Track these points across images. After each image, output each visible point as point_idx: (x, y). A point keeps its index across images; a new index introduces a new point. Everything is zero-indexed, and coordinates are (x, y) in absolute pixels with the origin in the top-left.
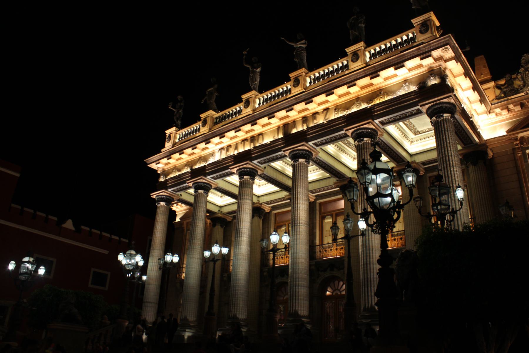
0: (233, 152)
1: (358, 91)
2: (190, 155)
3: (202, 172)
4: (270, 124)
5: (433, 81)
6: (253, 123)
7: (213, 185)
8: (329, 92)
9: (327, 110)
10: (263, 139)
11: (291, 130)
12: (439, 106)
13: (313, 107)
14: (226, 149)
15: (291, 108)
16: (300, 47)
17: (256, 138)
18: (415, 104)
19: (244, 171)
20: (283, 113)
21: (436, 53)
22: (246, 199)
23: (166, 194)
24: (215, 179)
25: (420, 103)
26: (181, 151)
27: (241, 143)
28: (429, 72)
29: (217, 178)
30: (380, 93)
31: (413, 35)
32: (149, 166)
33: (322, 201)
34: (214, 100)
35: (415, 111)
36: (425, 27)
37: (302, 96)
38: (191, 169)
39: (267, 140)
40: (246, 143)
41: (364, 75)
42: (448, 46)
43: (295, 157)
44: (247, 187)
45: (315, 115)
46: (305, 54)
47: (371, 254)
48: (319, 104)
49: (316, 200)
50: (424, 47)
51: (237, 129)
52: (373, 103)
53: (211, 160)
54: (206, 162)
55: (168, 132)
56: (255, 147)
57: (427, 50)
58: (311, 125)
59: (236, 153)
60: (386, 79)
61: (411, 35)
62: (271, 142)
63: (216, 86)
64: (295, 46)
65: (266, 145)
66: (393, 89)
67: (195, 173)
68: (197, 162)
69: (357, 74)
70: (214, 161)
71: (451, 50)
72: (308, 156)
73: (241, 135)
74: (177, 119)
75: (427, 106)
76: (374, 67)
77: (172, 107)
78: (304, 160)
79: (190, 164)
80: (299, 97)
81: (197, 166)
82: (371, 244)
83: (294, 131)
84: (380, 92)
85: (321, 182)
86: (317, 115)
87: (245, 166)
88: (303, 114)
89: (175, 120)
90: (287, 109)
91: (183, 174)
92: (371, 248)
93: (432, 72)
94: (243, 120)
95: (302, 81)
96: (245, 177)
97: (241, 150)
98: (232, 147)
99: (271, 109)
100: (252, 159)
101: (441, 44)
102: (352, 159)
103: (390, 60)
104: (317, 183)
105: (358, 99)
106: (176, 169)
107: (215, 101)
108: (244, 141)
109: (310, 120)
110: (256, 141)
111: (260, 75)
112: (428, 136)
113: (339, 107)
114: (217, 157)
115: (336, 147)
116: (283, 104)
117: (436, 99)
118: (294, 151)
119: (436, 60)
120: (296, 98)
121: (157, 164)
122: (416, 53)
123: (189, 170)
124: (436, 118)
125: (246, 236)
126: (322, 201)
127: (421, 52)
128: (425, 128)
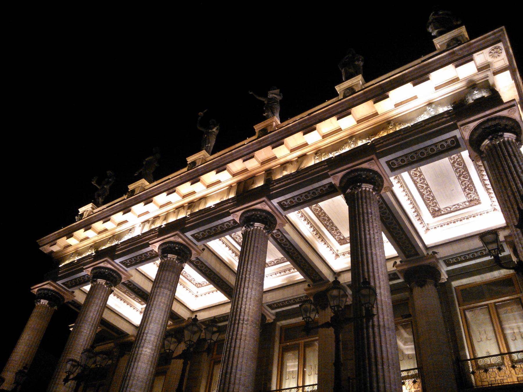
1: (354, 127)
3: (111, 253)
6: (195, 180)
12: (494, 123)
15: (251, 155)
19: (170, 247)
22: (165, 288)
23: (52, 288)
28: (468, 88)
32: (41, 248)
33: (284, 322)
35: (449, 142)
37: (268, 137)
39: (211, 203)
40: (182, 210)
42: (500, 45)
44: (170, 271)
47: (380, 373)
49: (275, 321)
50: (461, 49)
52: (377, 137)
55: (81, 210)
57: (466, 53)
73: (175, 199)
74: (99, 196)
75: (472, 126)
77: (96, 183)
78: (263, 226)
82: (379, 355)
86: (287, 165)
87: (172, 239)
88: (267, 166)
89: (96, 197)
90: (245, 158)
92: (379, 359)
93: (472, 85)
94: (181, 177)
96: (169, 256)
99: (221, 159)
101: (489, 43)
102: (334, 255)
103: (406, 74)
104: (281, 292)
112: (453, 219)
114: (137, 232)
115: (312, 229)
116: (240, 150)
117: (488, 112)
118: (248, 211)
124: (491, 140)
125: (150, 347)
126: (284, 322)
128: (450, 204)
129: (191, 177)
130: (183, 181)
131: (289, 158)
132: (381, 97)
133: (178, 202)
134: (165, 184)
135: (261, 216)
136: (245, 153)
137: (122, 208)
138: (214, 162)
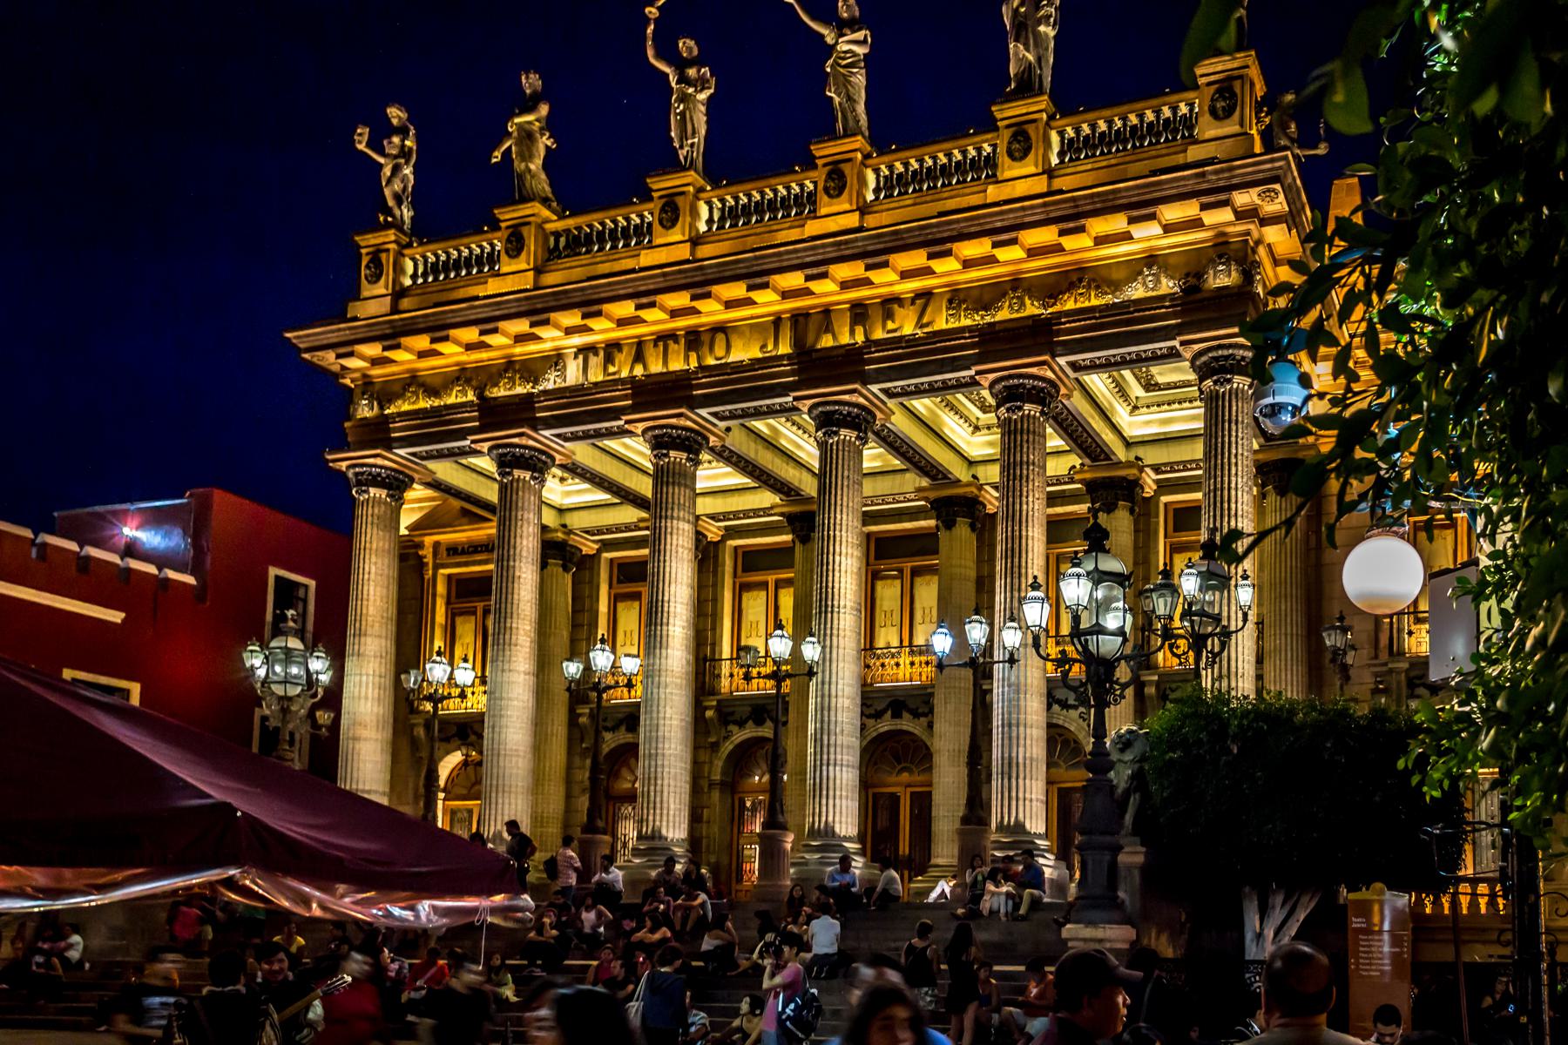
0: (623, 368)
2: (469, 347)
4: (749, 302)
5: (1222, 278)
7: (558, 457)
8: (937, 243)
9: (926, 296)
10: (728, 348)
11: (817, 338)
12: (1225, 352)
13: (886, 280)
14: (602, 353)
16: (849, 51)
17: (706, 338)
18: (1167, 334)
20: (795, 280)
21: (1242, 199)
24: (566, 439)
25: (1180, 334)
26: (438, 330)
27: (656, 342)
29: (575, 437)
30: (1080, 280)
31: (1191, 111)
34: (539, 161)
36: (1226, 98)
38: (481, 396)
39: (743, 352)
41: (1042, 217)
43: (827, 421)
45: (889, 304)
46: (860, 79)
48: (905, 275)
53: (551, 382)
54: (536, 382)
56: (701, 368)
58: (879, 334)
59: (639, 371)
60: (1100, 241)
61: (1183, 109)
62: (756, 363)
63: (544, 110)
64: (830, 40)
65: (738, 367)
66: (1117, 275)
67: (495, 415)
68: (501, 376)
69: (1023, 209)
70: (560, 384)
71: (1282, 196)
72: (862, 421)
76: (1074, 199)
78: (854, 434)
81: (500, 392)
83: (827, 341)
84: (1076, 277)
89: (391, 203)
91: (447, 407)
93: (1223, 249)
95: (851, 180)
98: (625, 349)
100: (694, 403)
105: (1016, 285)
106: (414, 382)
107: (546, 166)
108: (665, 338)
109: (876, 315)
110: (706, 349)
111: (708, 114)
113: (962, 296)
114: (573, 373)
119: (1240, 215)
121: (339, 356)
123: (471, 396)
124: (1215, 383)
131: (898, 288)
135: (849, 413)
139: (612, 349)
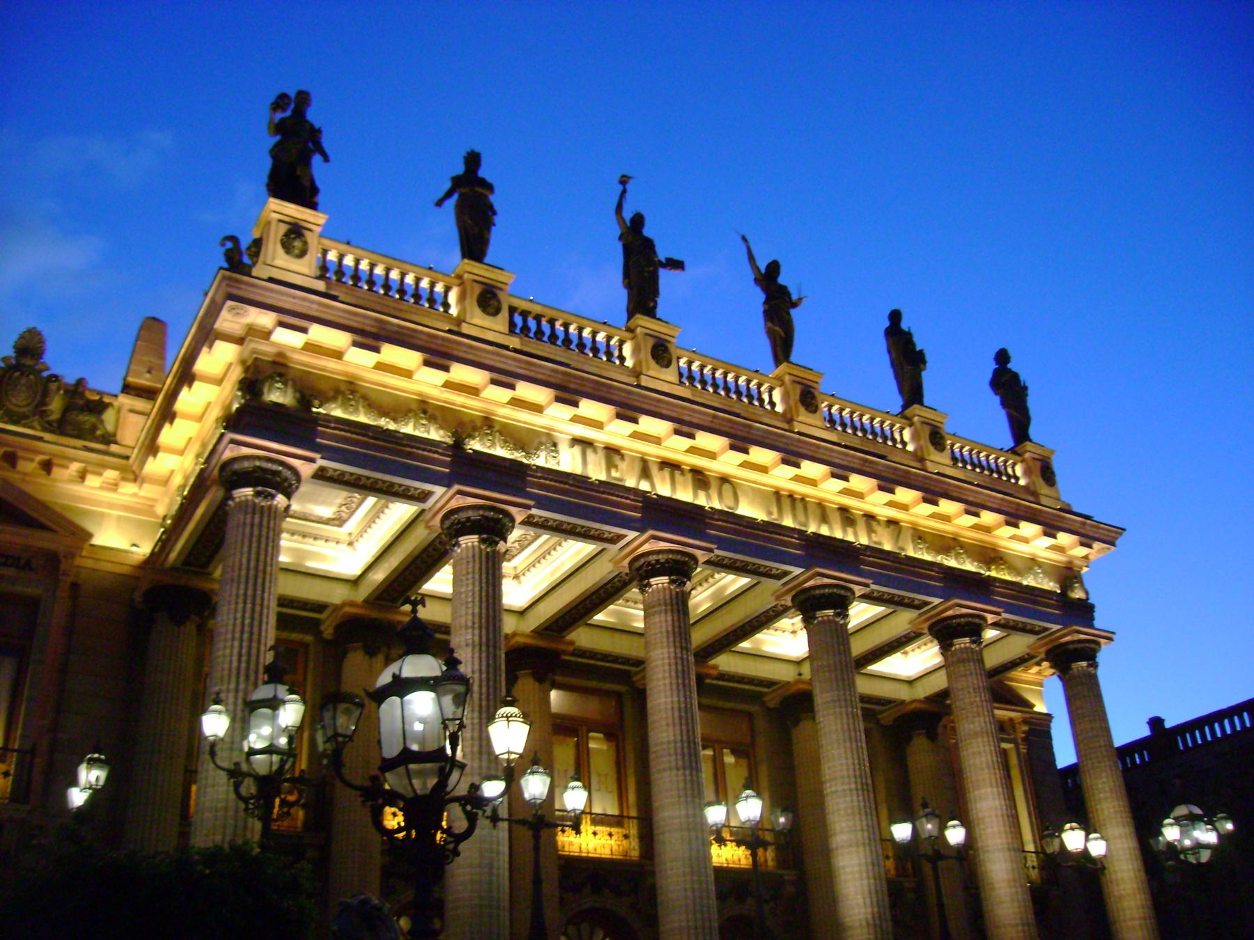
6: (739, 444)
38: (458, 446)
50: (1092, 526)
51: (685, 429)
53: (541, 460)
54: (528, 454)
79: (462, 427)
80: (871, 462)
81: (475, 445)
85: (617, 635)
90: (836, 471)
94: (715, 417)
97: (662, 488)
99: (799, 441)
108: (671, 466)
114: (568, 461)
116: (832, 451)
120: (866, 461)
122: (1076, 527)
123: (435, 434)
127: (1083, 531)
129: (732, 431)
130: (713, 426)
132: (1013, 520)
133: (677, 451)
134: (677, 406)
136: (837, 461)
137: (552, 380)
138: (783, 436)
139: (612, 452)
